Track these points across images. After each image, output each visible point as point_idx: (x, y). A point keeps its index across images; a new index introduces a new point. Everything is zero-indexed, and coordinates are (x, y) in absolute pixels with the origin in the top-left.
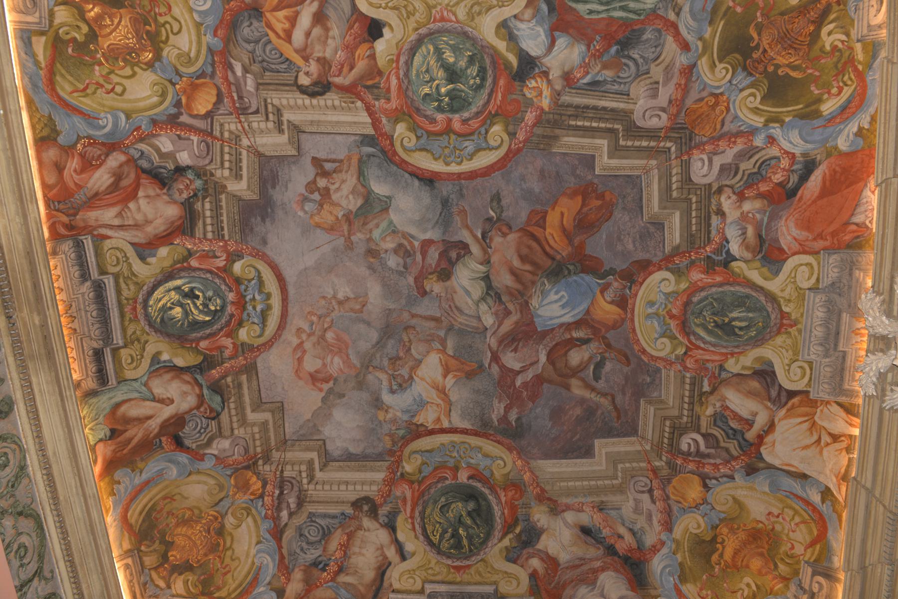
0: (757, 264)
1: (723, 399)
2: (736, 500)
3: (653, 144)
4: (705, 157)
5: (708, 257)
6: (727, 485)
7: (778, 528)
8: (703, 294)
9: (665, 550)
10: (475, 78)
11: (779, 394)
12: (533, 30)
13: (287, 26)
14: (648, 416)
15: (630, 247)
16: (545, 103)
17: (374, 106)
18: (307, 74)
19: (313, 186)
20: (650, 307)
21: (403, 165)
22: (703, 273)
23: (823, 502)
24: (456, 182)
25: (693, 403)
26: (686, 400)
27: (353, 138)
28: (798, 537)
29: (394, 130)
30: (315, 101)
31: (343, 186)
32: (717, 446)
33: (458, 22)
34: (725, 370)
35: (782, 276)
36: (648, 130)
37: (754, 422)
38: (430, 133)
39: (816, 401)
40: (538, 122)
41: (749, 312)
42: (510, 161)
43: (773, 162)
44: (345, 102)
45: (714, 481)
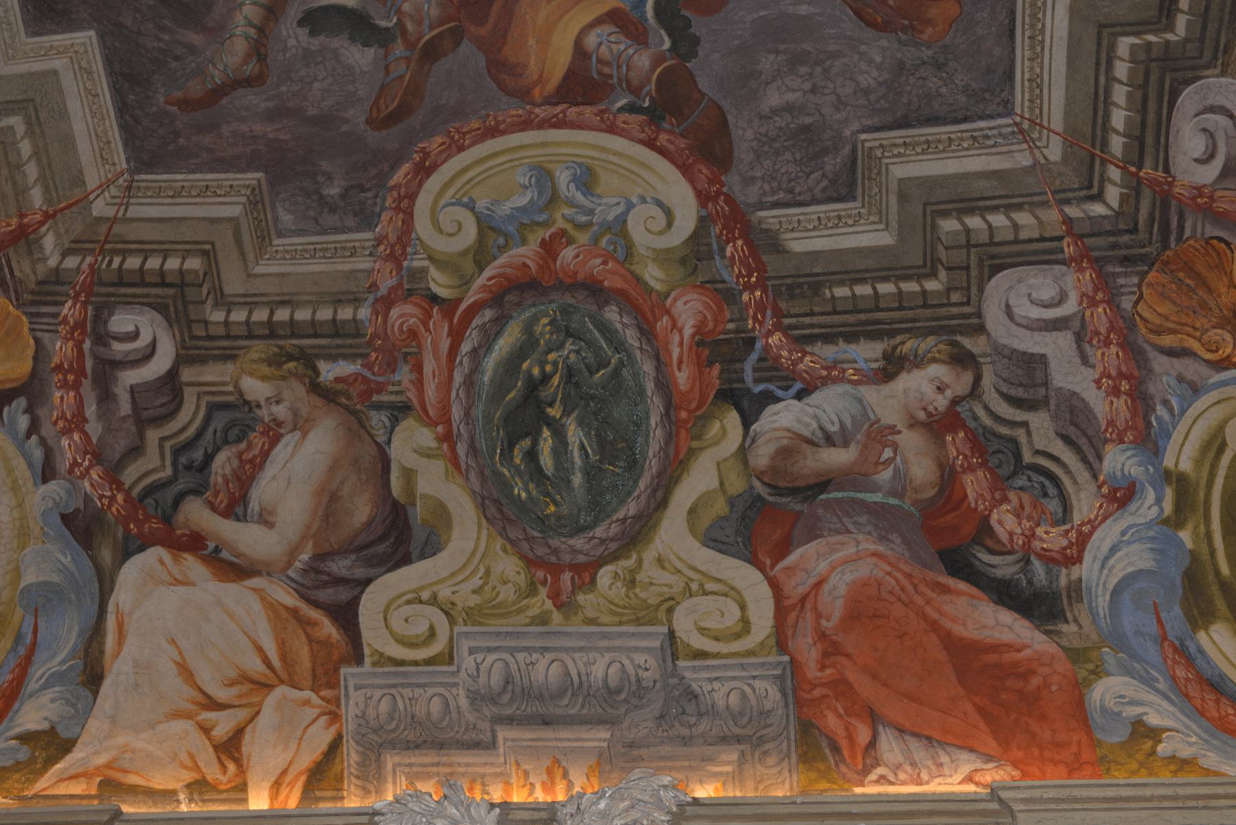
0: (737, 485)
1: (301, 425)
3: (1117, 144)
4: (1070, 307)
5: (750, 343)
6: (20, 464)
8: (631, 337)
11: (338, 581)
14: (207, 200)
15: (773, 98)
20: (574, 179)
22: (699, 329)
25: (272, 335)
26: (282, 315)
32: (142, 421)
34: (395, 421)
35: (706, 558)
36: (1164, 125)
37: (243, 518)
39: (333, 684)
41: (587, 474)
43: (1053, 505)
45: (23, 422)
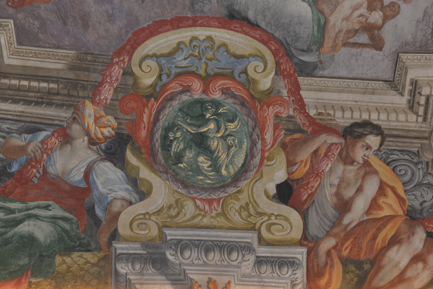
10: (175, 138)
12: (110, 190)
13: (381, 200)
16: (89, 109)
17: (295, 109)
18: (368, 147)
19: (389, 13)
21: (266, 38)
24: (198, 15)
27: (326, 73)
29: (273, 81)
30: (365, 116)
31: (348, 12)
33: (194, 199)
38: (231, 76)
40: (97, 87)
42: (129, 40)
44: (329, 115)
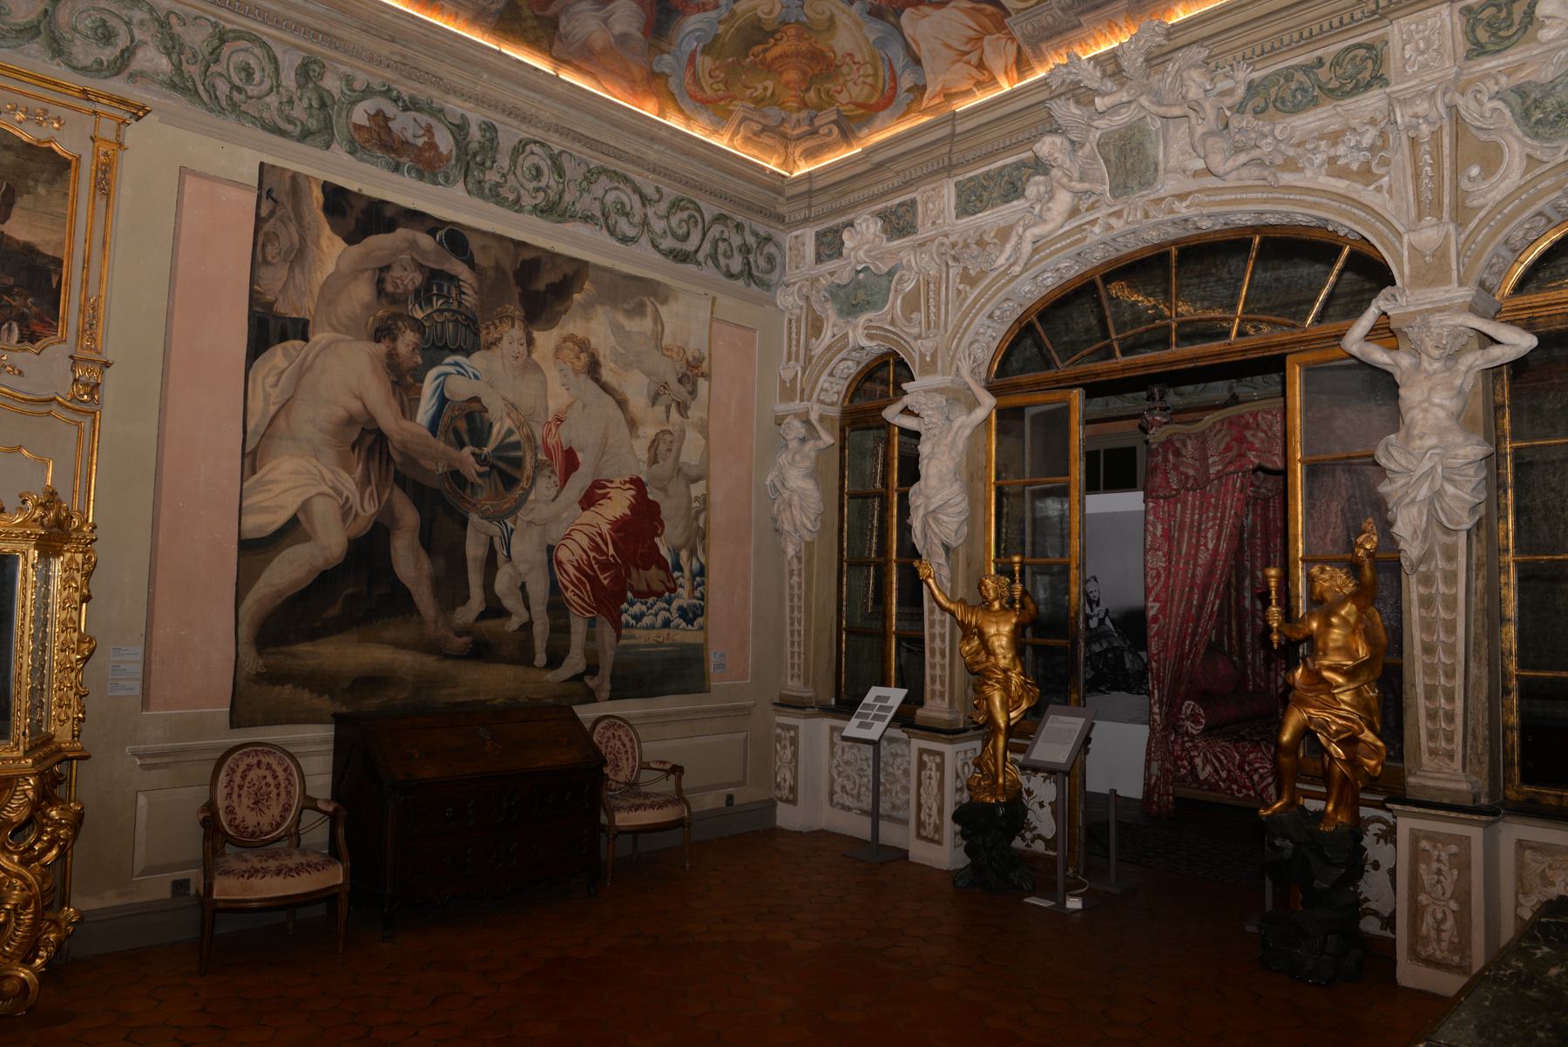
2: (832, 20)
7: (845, 69)
9: (712, 14)
23: (909, 90)
28: (853, 90)
39: (1005, 27)
